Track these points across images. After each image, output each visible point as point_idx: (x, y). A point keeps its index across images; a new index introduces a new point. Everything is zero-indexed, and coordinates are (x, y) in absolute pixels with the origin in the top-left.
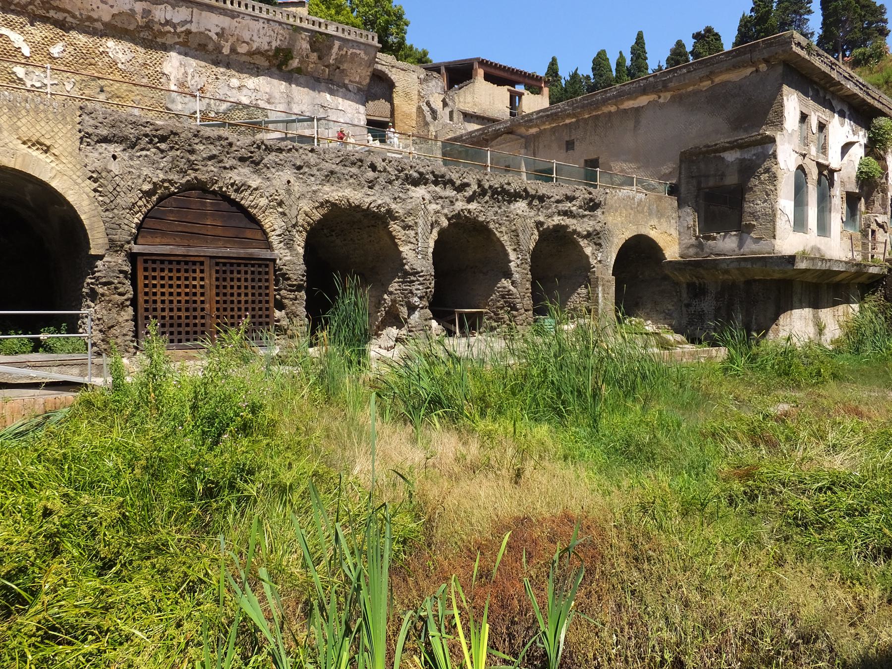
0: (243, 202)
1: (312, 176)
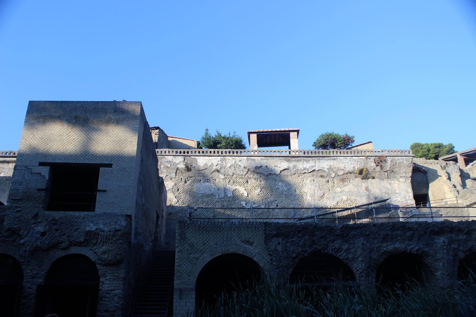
0: (340, 257)
1: (376, 238)
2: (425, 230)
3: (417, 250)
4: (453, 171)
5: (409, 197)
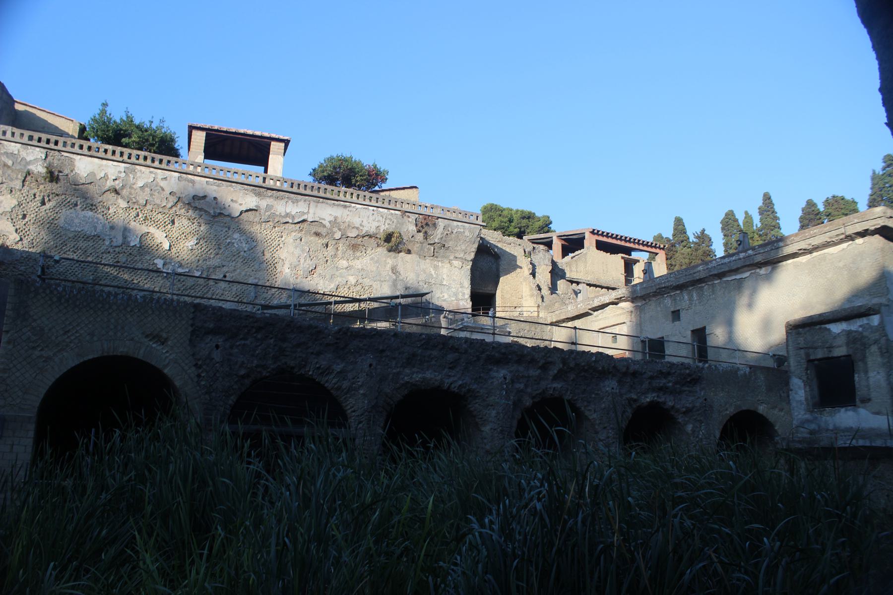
0: (326, 385)
1: (394, 359)
2: (478, 354)
3: (460, 385)
4: (542, 263)
5: (464, 294)
